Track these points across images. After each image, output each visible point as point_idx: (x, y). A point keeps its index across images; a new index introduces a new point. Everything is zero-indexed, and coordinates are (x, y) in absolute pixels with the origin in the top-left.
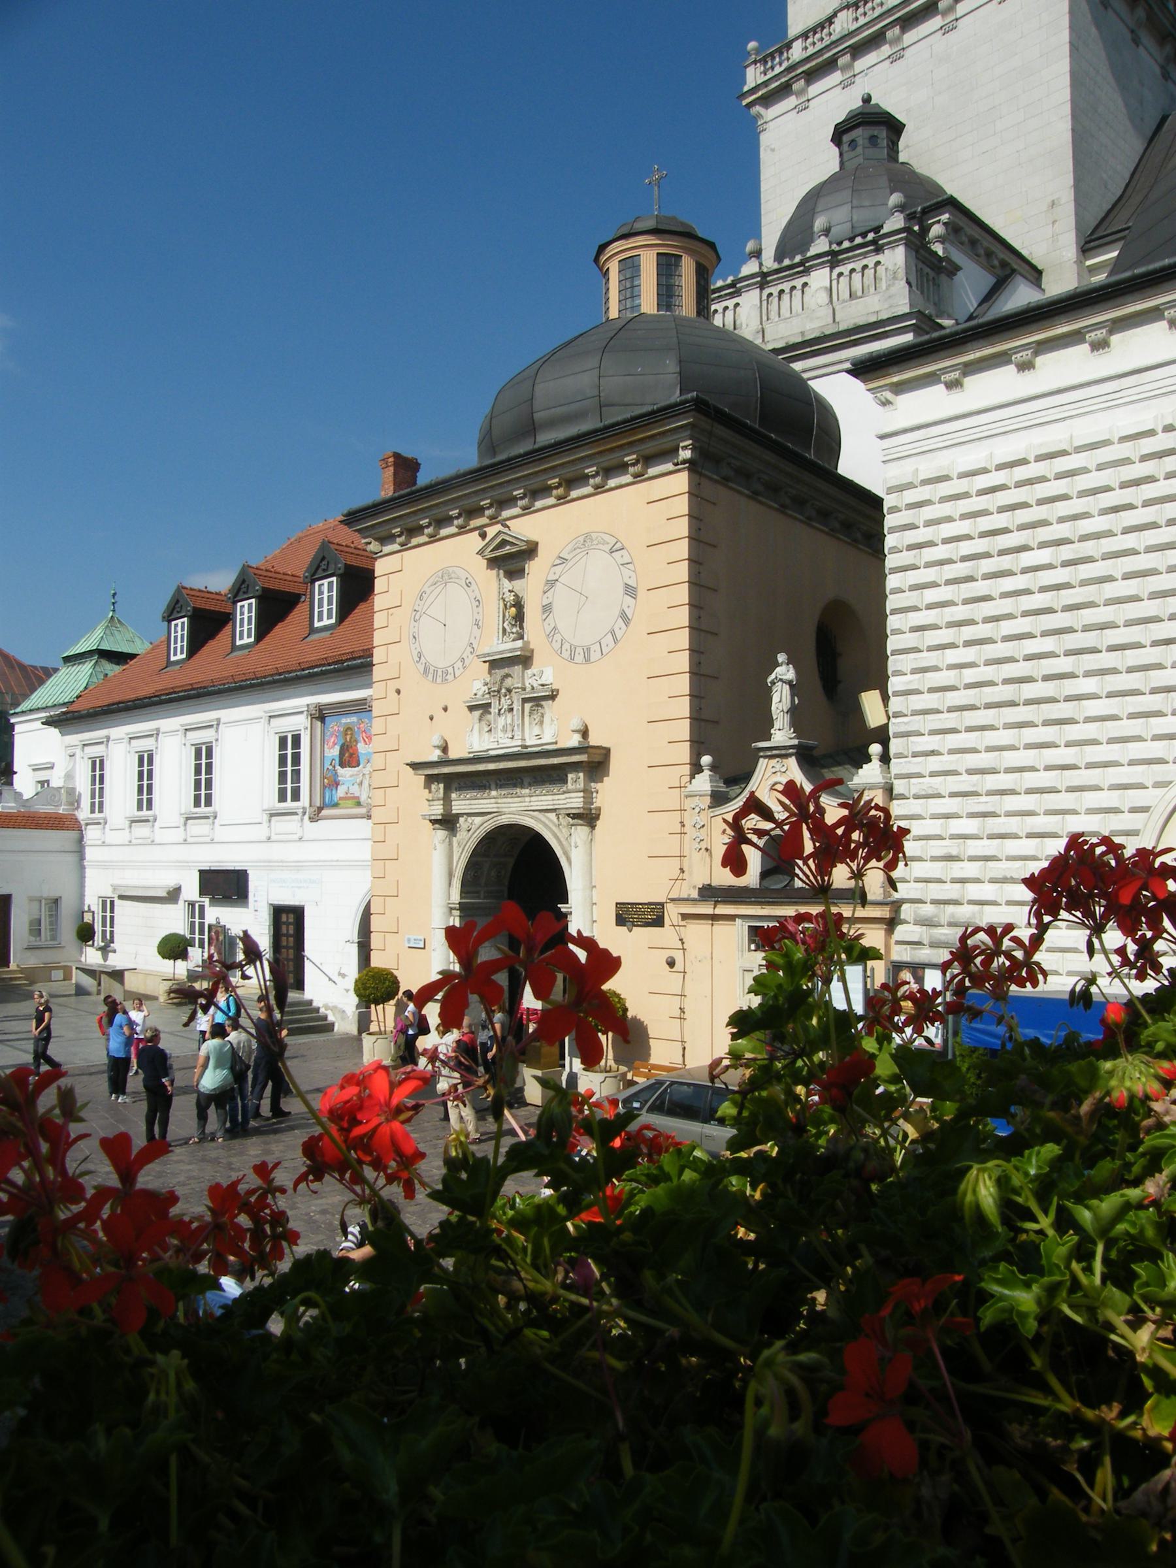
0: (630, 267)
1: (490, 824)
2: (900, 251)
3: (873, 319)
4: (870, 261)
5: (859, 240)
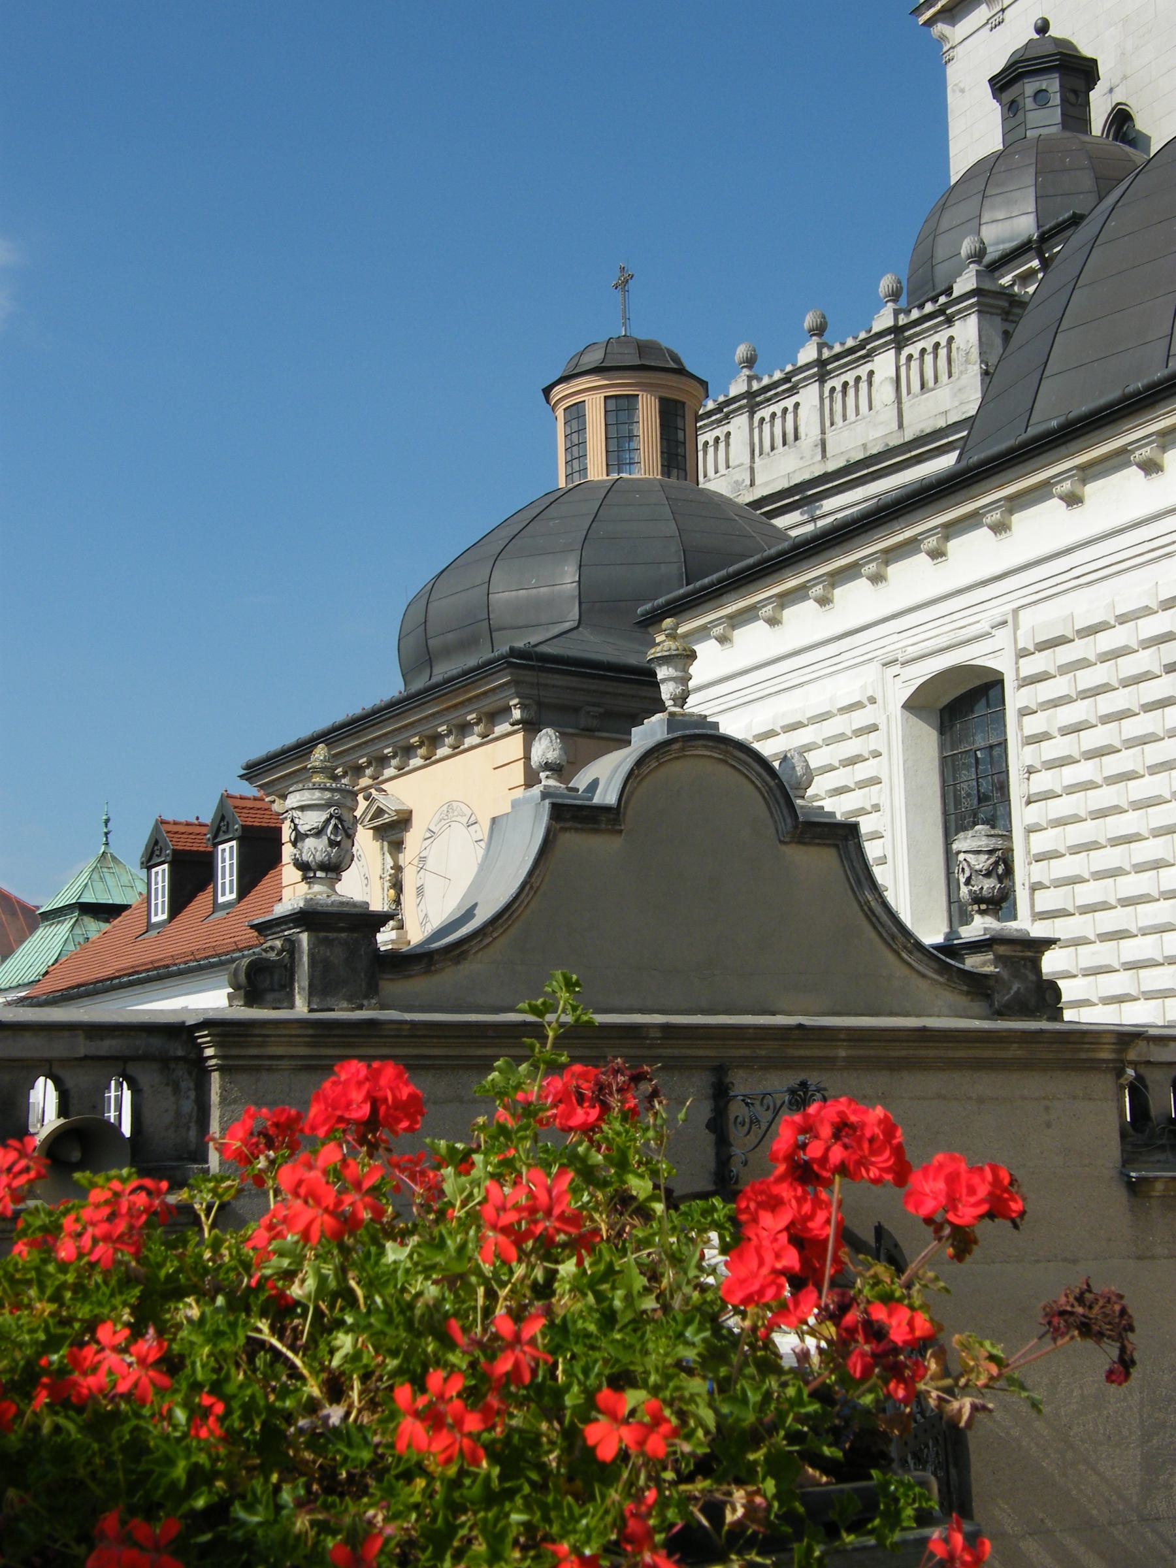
0: (576, 414)
2: (973, 320)
3: (941, 423)
4: (942, 337)
5: (929, 308)
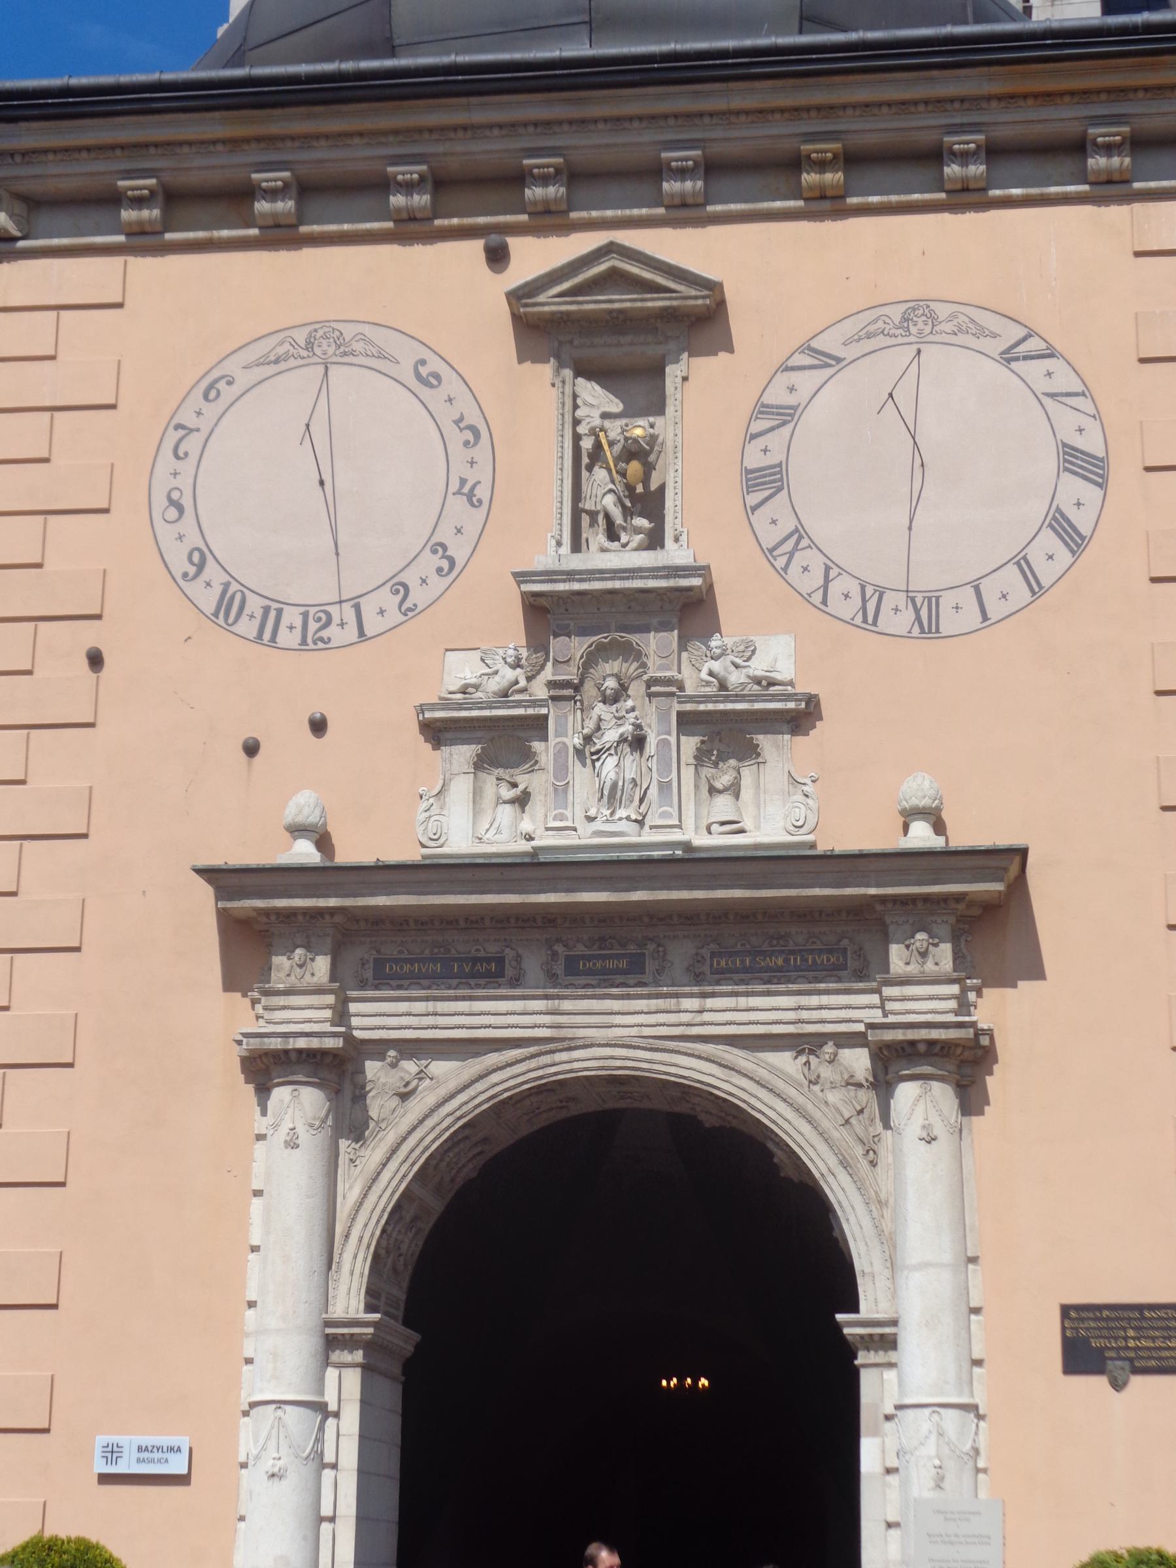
1: (510, 1075)
